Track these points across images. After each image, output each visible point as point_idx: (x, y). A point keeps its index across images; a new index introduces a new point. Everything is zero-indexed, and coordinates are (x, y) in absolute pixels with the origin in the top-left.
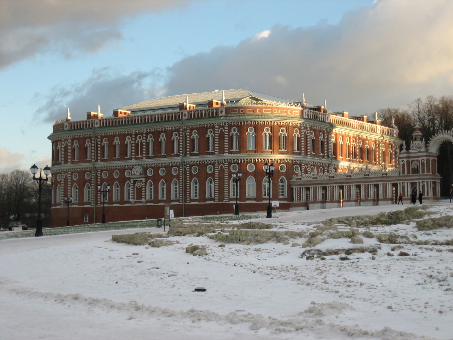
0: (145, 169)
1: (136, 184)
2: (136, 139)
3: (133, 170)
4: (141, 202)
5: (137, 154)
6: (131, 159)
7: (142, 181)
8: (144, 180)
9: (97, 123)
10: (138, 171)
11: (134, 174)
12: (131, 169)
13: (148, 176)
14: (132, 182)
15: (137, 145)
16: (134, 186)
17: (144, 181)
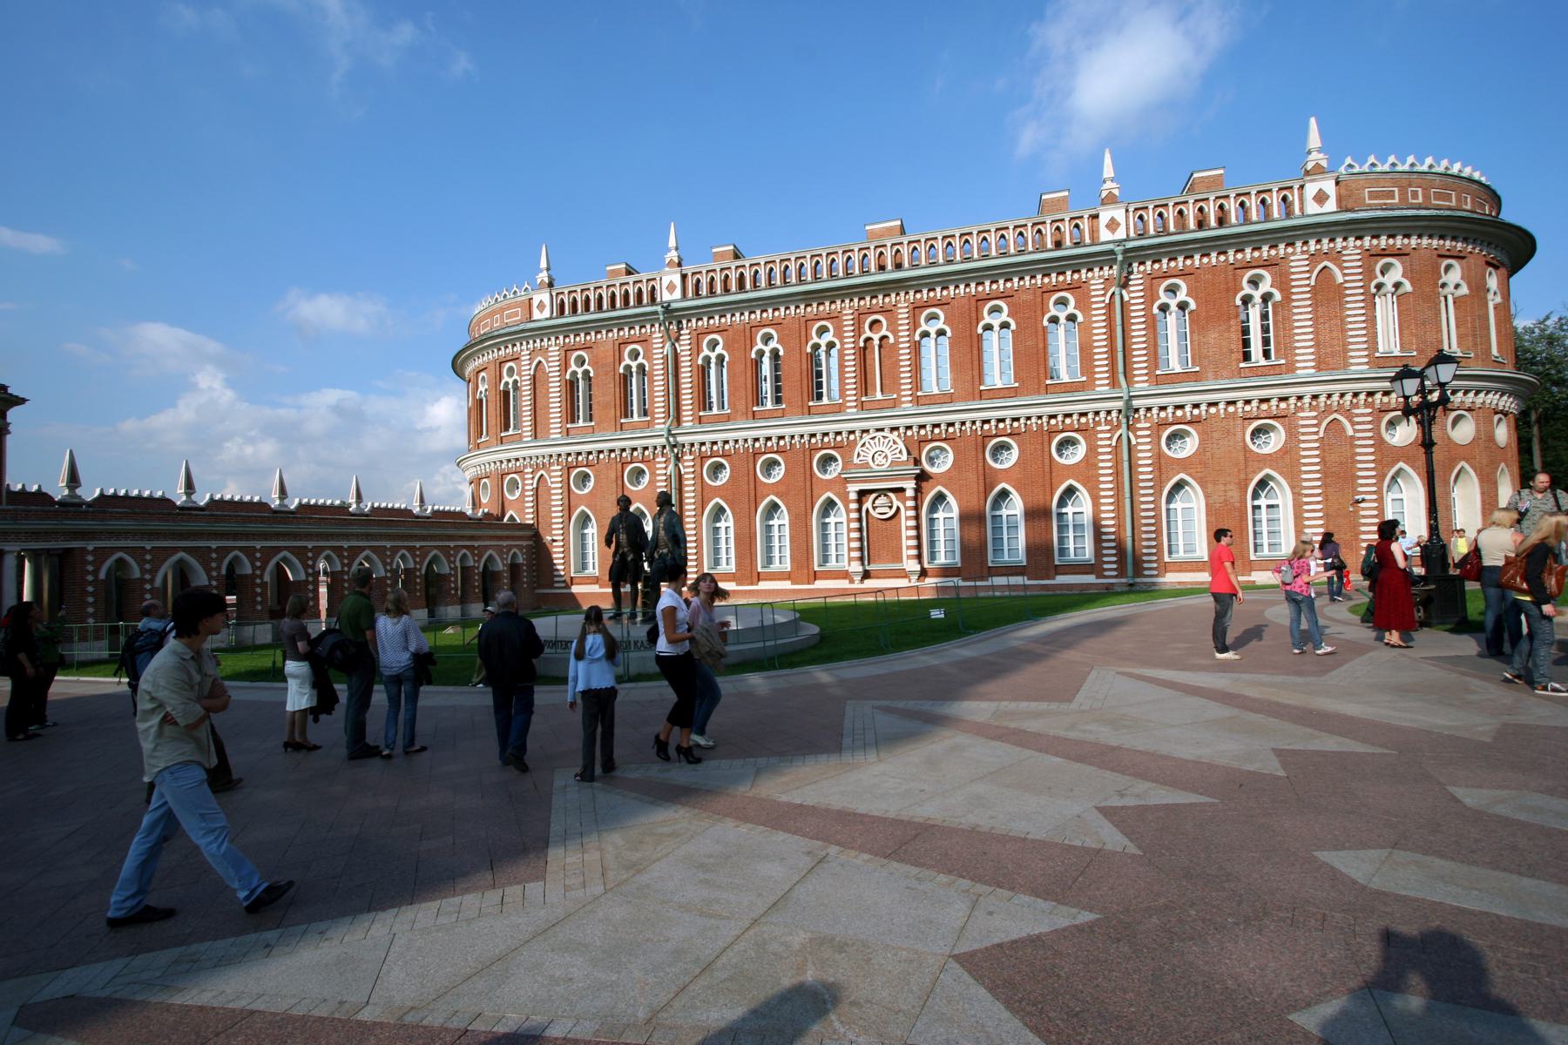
0: (914, 447)
1: (868, 505)
2: (858, 331)
3: (858, 449)
4: (904, 574)
5: (865, 385)
6: (839, 409)
7: (902, 490)
8: (910, 485)
9: (671, 288)
10: (882, 453)
11: (866, 465)
12: (847, 448)
13: (923, 471)
14: (853, 496)
15: (863, 353)
16: (859, 510)
17: (910, 493)
